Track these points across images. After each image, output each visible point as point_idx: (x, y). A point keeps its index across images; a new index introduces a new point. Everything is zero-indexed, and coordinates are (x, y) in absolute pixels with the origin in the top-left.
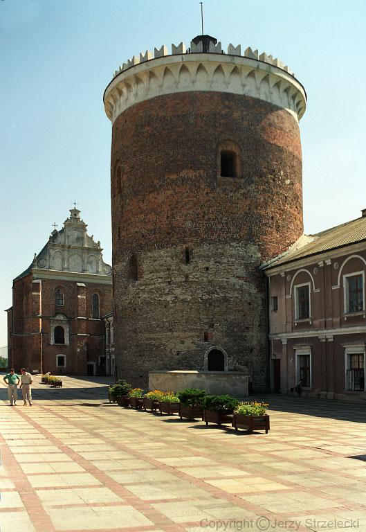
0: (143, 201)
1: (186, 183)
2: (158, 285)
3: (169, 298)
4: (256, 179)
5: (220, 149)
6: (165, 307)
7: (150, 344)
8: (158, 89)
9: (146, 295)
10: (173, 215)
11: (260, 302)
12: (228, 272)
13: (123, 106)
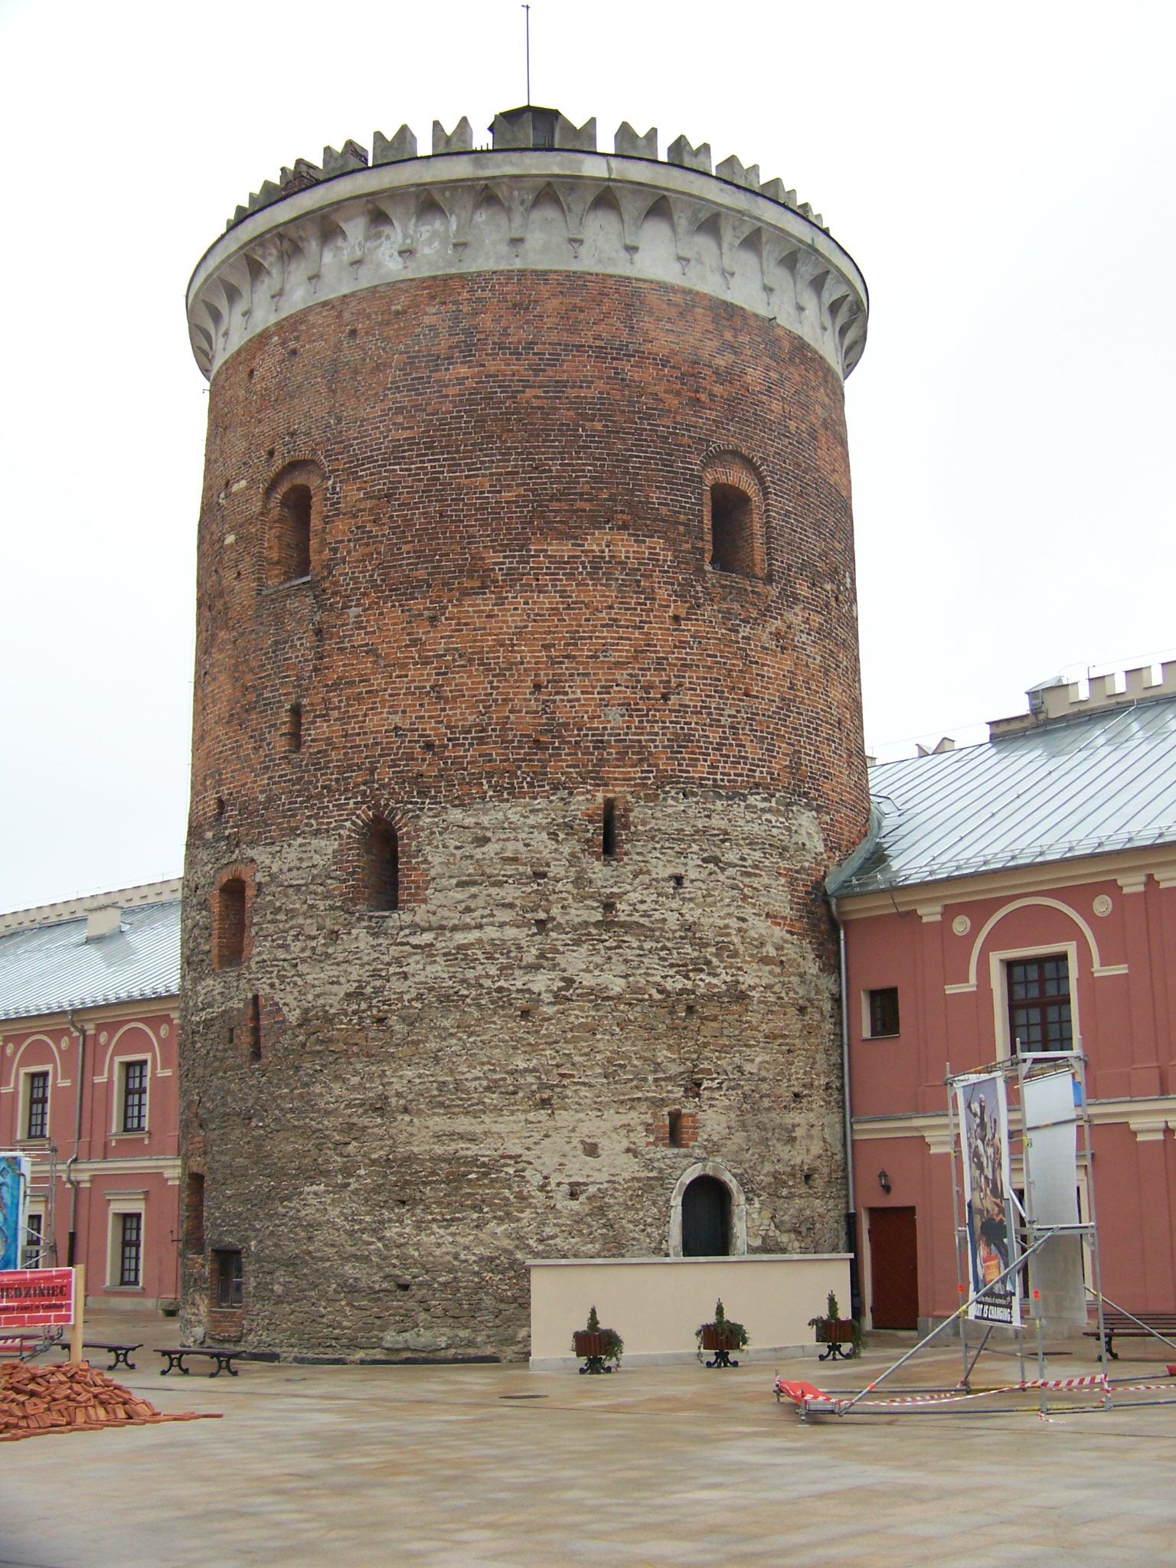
0: (433, 619)
1: (608, 575)
2: (491, 932)
3: (541, 982)
4: (803, 590)
5: (709, 478)
6: (525, 1014)
7: (452, 1159)
8: (504, 249)
10: (555, 681)
11: (827, 1006)
12: (745, 898)
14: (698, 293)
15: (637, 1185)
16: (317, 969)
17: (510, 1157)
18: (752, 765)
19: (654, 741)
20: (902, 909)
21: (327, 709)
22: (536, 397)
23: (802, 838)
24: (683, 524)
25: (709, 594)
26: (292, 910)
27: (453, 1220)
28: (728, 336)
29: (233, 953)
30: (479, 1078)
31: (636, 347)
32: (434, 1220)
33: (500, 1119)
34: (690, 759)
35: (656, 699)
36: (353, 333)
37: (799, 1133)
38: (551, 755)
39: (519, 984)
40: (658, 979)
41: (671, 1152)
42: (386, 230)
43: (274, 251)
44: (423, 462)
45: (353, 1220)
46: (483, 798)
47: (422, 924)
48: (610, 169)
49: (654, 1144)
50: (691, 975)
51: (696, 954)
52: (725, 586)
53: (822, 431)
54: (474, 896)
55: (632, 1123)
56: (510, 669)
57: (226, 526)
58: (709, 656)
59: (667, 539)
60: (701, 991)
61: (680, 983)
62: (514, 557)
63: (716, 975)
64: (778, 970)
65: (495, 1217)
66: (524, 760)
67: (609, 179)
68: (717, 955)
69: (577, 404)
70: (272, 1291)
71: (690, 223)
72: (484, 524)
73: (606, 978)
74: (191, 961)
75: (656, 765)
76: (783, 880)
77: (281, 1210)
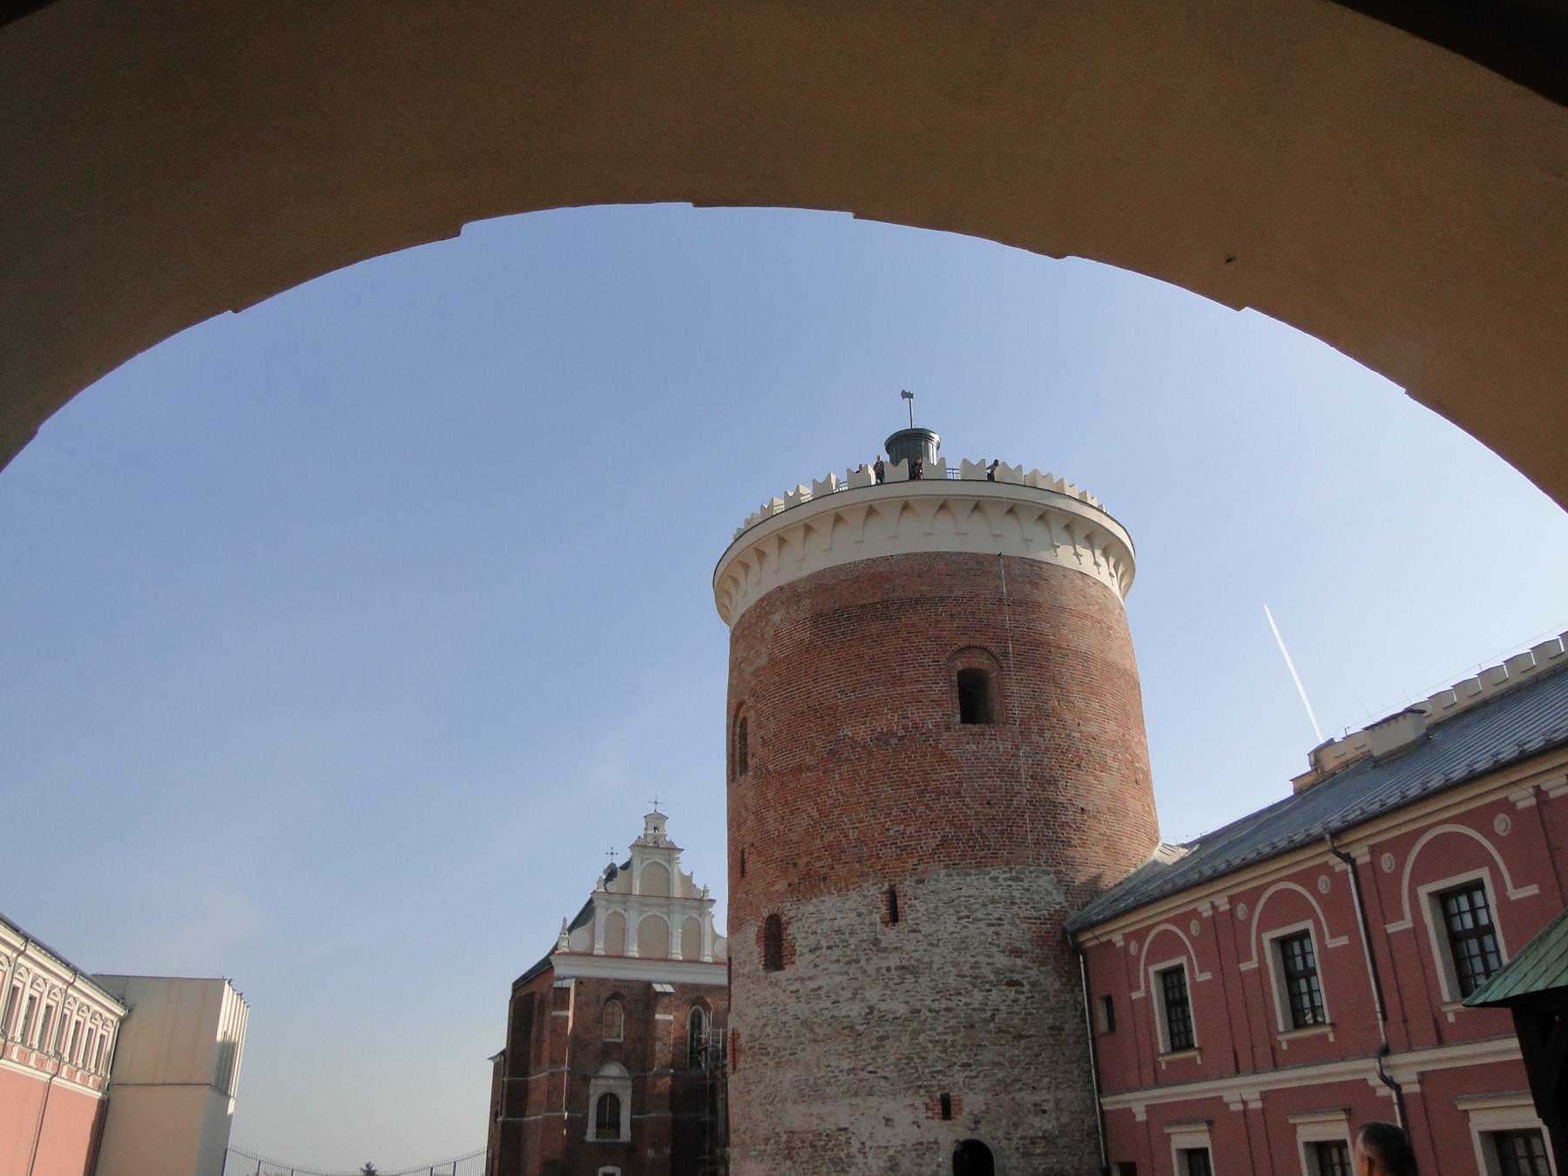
9: (802, 1009)
13: (751, 592)
20: (1103, 939)
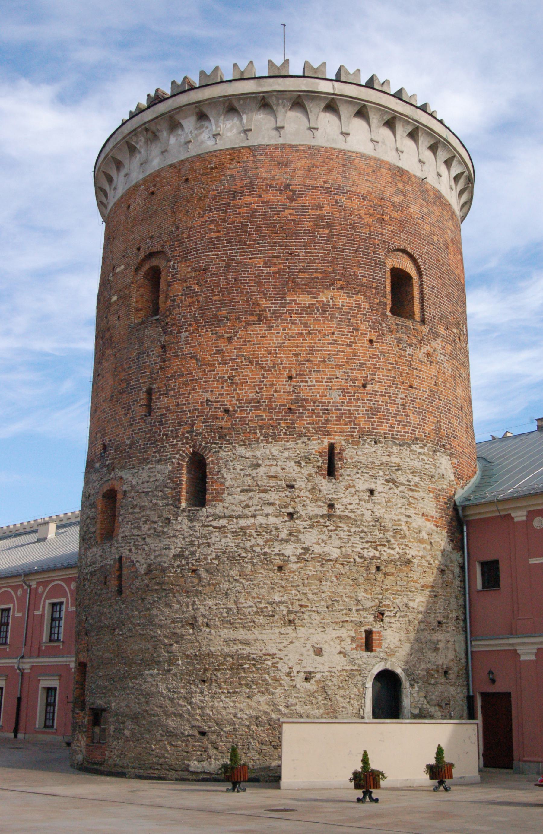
0: (230, 339)
1: (332, 315)
2: (260, 520)
3: (290, 550)
4: (442, 330)
9: (229, 541)
11: (457, 570)
12: (410, 504)
14: (383, 161)
15: (345, 674)
16: (157, 541)
17: (269, 655)
18: (415, 427)
19: (357, 410)
20: (502, 513)
21: (167, 390)
22: (290, 214)
23: (442, 471)
24: (375, 288)
25: (390, 328)
26: (143, 506)
27: (235, 692)
28: (400, 185)
29: (109, 534)
30: (251, 607)
31: (348, 188)
32: (223, 692)
33: (264, 632)
34: (378, 422)
35: (358, 386)
36: (187, 180)
37: (441, 645)
38: (298, 417)
39: (276, 551)
40: (359, 550)
41: (365, 654)
42: (206, 124)
43: (143, 139)
44: (226, 250)
45: (174, 692)
46: (257, 441)
47: (220, 514)
48: (334, 88)
49: (356, 649)
50: (379, 548)
51: (381, 535)
52: (399, 325)
53: (451, 245)
54: (251, 498)
55: (343, 635)
56: (274, 367)
57: (112, 291)
58: (389, 363)
59: (366, 296)
60: (385, 557)
61: (372, 553)
62: (277, 303)
63: (393, 549)
64: (429, 547)
65: (259, 692)
66: (281, 419)
67: (334, 94)
68: (394, 537)
69: (315, 219)
70: (124, 734)
71: (379, 121)
72: (260, 284)
73: (327, 549)
74: (83, 539)
75: (359, 425)
76: (431, 495)
77: (131, 685)
